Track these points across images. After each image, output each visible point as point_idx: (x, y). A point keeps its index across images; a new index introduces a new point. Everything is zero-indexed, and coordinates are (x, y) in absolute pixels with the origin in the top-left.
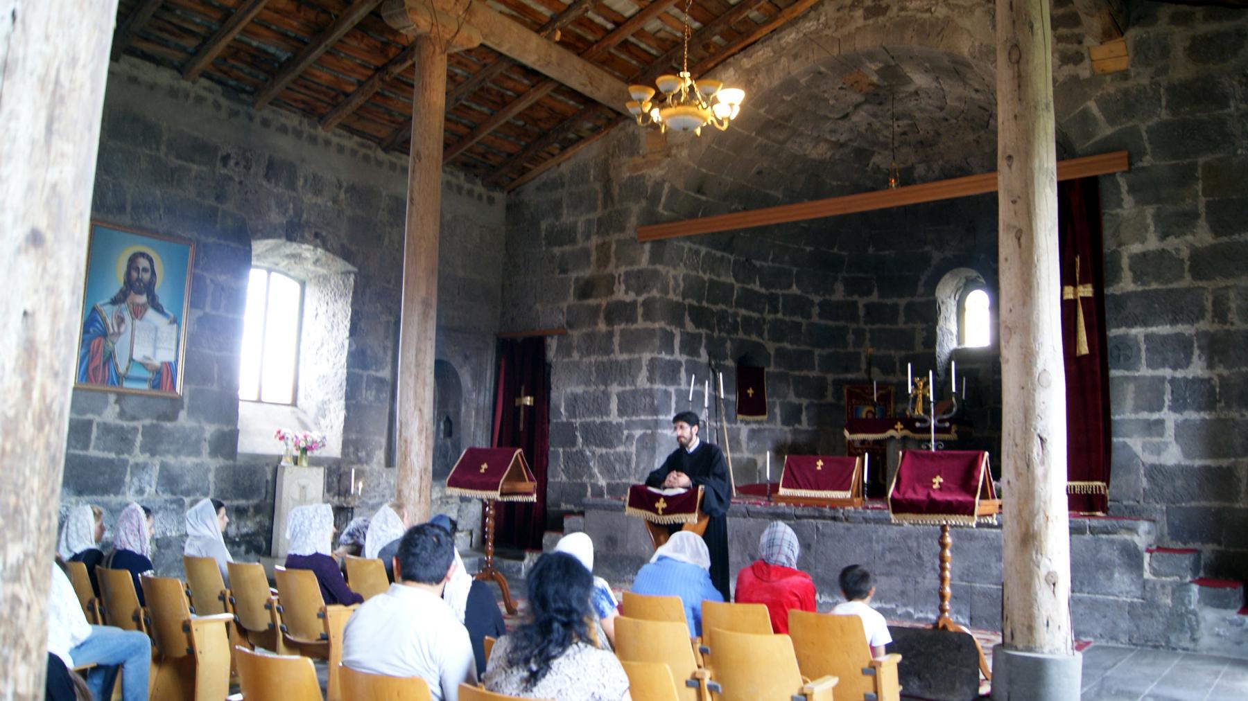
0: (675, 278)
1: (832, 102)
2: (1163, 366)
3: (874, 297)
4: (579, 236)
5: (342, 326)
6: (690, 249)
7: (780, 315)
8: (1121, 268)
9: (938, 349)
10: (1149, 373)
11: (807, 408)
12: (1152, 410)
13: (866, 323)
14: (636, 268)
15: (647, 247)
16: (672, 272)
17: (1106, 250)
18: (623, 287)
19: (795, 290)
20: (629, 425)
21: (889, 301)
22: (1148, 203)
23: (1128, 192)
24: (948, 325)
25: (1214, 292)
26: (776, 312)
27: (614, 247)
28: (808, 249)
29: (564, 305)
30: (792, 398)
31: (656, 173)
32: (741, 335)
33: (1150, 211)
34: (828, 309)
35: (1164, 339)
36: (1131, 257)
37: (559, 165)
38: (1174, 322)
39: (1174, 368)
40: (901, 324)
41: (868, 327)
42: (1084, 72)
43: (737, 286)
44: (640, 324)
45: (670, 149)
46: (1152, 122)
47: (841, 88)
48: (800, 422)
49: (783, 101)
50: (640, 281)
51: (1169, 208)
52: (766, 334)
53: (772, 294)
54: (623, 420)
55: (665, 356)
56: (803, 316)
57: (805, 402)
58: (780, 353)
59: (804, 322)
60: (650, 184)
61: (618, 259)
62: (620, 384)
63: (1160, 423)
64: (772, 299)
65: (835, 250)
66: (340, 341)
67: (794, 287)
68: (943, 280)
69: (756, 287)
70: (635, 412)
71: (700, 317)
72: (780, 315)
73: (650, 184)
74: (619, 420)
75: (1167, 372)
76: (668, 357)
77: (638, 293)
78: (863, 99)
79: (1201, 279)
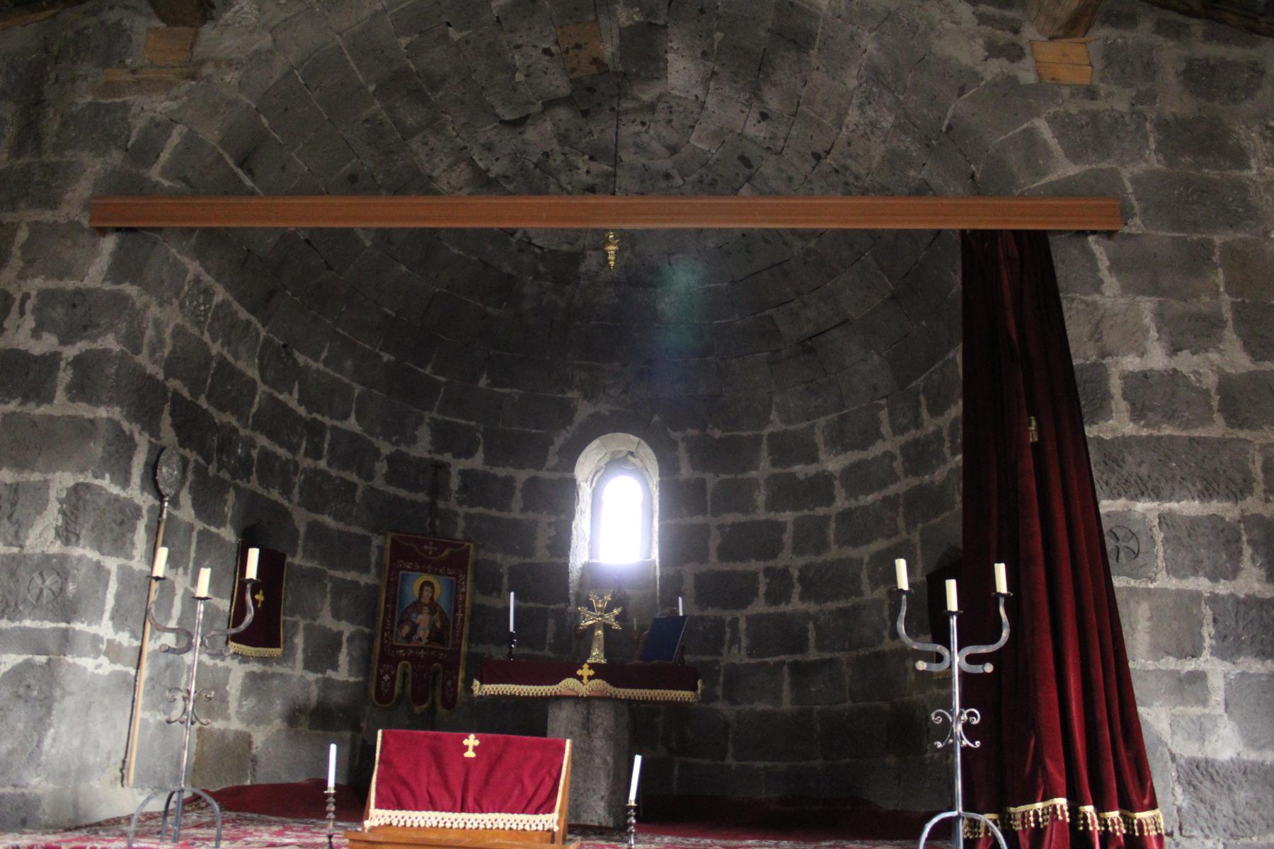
0: (158, 324)
1: (519, 77)
2: (1195, 572)
3: (477, 462)
6: (197, 280)
7: (322, 464)
8: (1107, 396)
9: (571, 560)
10: (1173, 584)
11: (351, 640)
12: (1182, 655)
13: (460, 503)
14: (70, 284)
15: (109, 244)
16: (154, 311)
18: (30, 322)
19: (352, 424)
21: (501, 472)
22: (1142, 292)
23: (1110, 269)
24: (581, 525)
25: (1263, 448)
26: (318, 456)
27: (23, 235)
28: (386, 357)
30: (327, 620)
31: (152, 106)
32: (254, 484)
34: (400, 468)
35: (1193, 524)
36: (1127, 377)
38: (1206, 494)
39: (1214, 577)
41: (462, 510)
43: (262, 388)
45: (202, 63)
46: (1139, 168)
47: (547, 52)
48: (335, 667)
49: (445, 37)
50: (77, 314)
51: (1177, 306)
52: (296, 490)
53: (314, 420)
55: (107, 484)
56: (359, 474)
57: (346, 628)
58: (315, 531)
59: (361, 484)
60: (139, 124)
61: (29, 263)
63: (1198, 678)
65: (428, 371)
67: (353, 419)
68: (588, 449)
69: (291, 400)
71: (192, 427)
72: (322, 464)
73: (139, 124)
75: (1201, 584)
76: (115, 490)
78: (565, 90)
79: (1241, 427)
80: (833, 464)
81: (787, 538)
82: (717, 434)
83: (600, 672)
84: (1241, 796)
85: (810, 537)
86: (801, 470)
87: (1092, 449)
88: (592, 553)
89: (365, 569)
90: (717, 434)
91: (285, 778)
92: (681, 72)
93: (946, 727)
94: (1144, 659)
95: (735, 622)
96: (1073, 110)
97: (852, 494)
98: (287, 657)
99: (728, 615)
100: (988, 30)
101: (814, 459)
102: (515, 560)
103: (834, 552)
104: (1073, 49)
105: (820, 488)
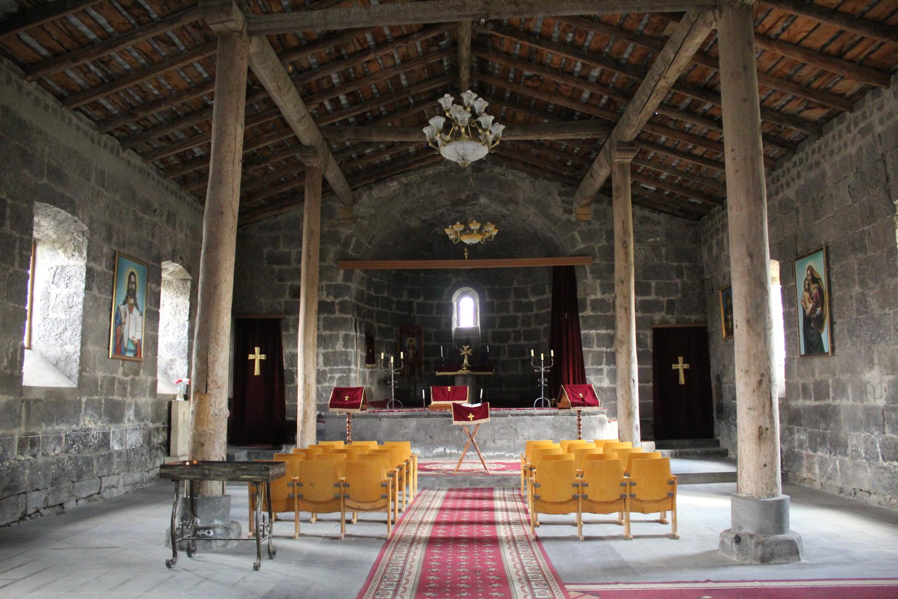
3: (421, 300)
4: (292, 260)
5: (183, 313)
8: (586, 305)
10: (598, 349)
14: (334, 283)
15: (342, 272)
17: (579, 297)
18: (325, 293)
19: (386, 294)
20: (331, 371)
21: (428, 302)
29: (283, 301)
31: (345, 232)
37: (276, 216)
38: (607, 329)
40: (434, 315)
41: (418, 315)
42: (573, 218)
44: (337, 315)
46: (600, 245)
51: (605, 282)
54: (327, 369)
60: (343, 237)
62: (324, 348)
63: (601, 370)
64: (377, 298)
66: (182, 321)
70: (335, 364)
74: (325, 368)
75: (604, 349)
77: (336, 297)
80: (533, 299)
81: (520, 321)
82: (497, 287)
83: (468, 368)
85: (526, 322)
86: (523, 300)
87: (581, 321)
88: (458, 324)
90: (497, 287)
91: (379, 400)
92: (483, 200)
93: (540, 383)
94: (588, 366)
95: (504, 347)
97: (539, 309)
99: (502, 345)
100: (564, 205)
101: (527, 297)
103: (533, 327)
104: (587, 210)
105: (529, 306)
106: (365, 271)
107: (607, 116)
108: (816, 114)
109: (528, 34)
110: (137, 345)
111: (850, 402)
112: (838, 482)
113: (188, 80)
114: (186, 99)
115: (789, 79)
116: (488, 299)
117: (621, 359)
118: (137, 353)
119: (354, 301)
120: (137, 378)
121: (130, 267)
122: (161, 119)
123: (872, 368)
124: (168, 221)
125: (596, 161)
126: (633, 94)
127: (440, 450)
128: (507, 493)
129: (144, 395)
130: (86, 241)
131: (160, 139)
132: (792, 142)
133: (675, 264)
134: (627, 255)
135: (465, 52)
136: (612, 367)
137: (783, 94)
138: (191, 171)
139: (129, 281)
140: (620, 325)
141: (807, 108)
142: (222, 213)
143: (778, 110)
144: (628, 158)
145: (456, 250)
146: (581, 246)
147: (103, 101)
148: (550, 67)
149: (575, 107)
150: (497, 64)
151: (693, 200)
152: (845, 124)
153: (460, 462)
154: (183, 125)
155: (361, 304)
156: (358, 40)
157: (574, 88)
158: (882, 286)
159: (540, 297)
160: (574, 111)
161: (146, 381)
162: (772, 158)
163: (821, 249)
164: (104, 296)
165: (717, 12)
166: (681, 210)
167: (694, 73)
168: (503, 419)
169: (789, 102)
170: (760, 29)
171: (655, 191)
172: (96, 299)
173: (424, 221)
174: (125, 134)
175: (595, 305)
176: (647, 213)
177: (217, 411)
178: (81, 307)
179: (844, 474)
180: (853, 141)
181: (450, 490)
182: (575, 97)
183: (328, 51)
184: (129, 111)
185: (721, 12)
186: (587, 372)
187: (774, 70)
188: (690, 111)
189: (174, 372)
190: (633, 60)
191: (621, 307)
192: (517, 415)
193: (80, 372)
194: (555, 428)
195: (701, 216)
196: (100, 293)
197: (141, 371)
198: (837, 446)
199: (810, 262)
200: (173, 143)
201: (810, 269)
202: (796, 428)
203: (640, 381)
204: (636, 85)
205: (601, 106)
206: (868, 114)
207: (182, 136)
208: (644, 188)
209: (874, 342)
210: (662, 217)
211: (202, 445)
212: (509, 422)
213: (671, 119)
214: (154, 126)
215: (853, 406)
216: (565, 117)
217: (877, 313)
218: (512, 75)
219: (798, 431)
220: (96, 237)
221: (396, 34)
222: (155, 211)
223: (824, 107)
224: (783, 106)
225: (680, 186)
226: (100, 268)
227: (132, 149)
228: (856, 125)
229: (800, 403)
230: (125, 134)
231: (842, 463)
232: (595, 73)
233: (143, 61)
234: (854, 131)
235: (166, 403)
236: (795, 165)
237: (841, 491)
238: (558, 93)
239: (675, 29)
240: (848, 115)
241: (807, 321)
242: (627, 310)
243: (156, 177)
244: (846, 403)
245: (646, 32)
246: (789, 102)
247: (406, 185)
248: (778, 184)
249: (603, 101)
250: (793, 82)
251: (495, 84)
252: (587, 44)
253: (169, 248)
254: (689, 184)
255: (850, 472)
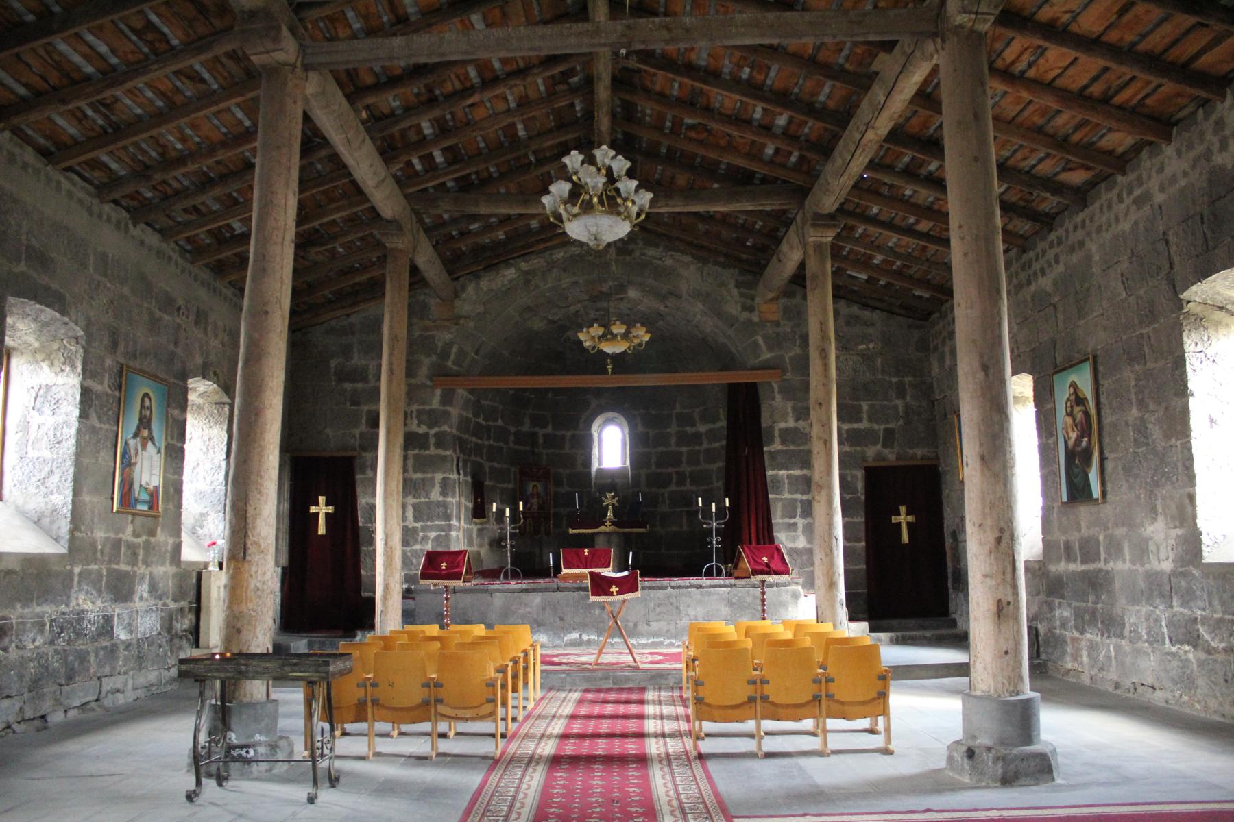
3: (549, 430)
4: (370, 377)
5: (217, 450)
14: (427, 407)
15: (438, 392)
17: (764, 425)
18: (415, 422)
19: (500, 422)
20: (424, 529)
29: (357, 432)
31: (444, 337)
33: (789, 405)
35: (797, 478)
36: (780, 430)
37: (348, 315)
38: (802, 468)
39: (802, 494)
40: (567, 450)
41: (545, 451)
44: (432, 451)
46: (791, 354)
51: (800, 404)
54: (419, 525)
58: (491, 468)
60: (440, 344)
62: (414, 497)
63: (795, 524)
64: (488, 428)
66: (216, 461)
70: (430, 519)
73: (440, 344)
74: (415, 525)
75: (798, 496)
77: (430, 428)
80: (702, 428)
83: (613, 523)
84: (804, 557)
86: (688, 429)
87: (766, 457)
88: (600, 463)
89: (509, 482)
90: (653, 412)
92: (633, 293)
93: (711, 543)
94: (777, 519)
95: (663, 494)
96: (770, 331)
98: (488, 522)
100: (742, 300)
101: (693, 425)
102: (568, 471)
105: (697, 438)
106: (472, 391)
107: (799, 180)
108: (1077, 177)
109: (689, 69)
110: (153, 494)
111: (1127, 566)
112: (1113, 674)
113: (224, 130)
114: (222, 155)
115: (1040, 130)
116: (640, 428)
117: (819, 509)
118: (153, 505)
119: (454, 431)
120: (152, 540)
121: (143, 387)
122: (186, 183)
123: (1155, 519)
124: (197, 323)
125: (784, 241)
126: (832, 150)
127: (575, 635)
128: (664, 695)
129: (163, 564)
130: (81, 351)
131: (185, 210)
132: (1047, 214)
133: (894, 380)
134: (826, 367)
135: (603, 92)
136: (809, 520)
137: (1033, 151)
138: (229, 254)
139: (142, 407)
140: (818, 463)
141: (1064, 170)
142: (267, 313)
143: (1028, 172)
144: (828, 237)
145: (597, 362)
146: (767, 355)
147: (105, 158)
148: (720, 114)
149: (754, 167)
150: (648, 109)
151: (917, 293)
152: (1116, 191)
153: (600, 653)
154: (218, 191)
155: (465, 436)
156: (458, 77)
157: (753, 142)
158: (1166, 408)
159: (711, 426)
160: (755, 172)
161: (166, 544)
162: (1021, 236)
163: (1087, 359)
164: (107, 426)
165: (939, 40)
166: (901, 306)
167: (914, 121)
168: (661, 593)
169: (1041, 160)
170: (999, 64)
171: (867, 281)
172: (94, 430)
173: (552, 322)
174: (135, 203)
175: (787, 436)
176: (855, 309)
177: (259, 585)
178: (73, 441)
179: (1121, 664)
180: (1126, 215)
181: (587, 691)
182: (755, 153)
183: (416, 90)
184: (143, 171)
185: (943, 41)
186: (775, 528)
187: (1020, 119)
188: (910, 173)
189: (206, 530)
190: (831, 104)
191: (819, 438)
192: (680, 587)
193: (72, 532)
194: (731, 604)
195: (930, 314)
196: (100, 422)
197: (159, 529)
198: (1111, 625)
199: (1073, 377)
200: (204, 215)
201: (1074, 385)
202: (1057, 601)
203: (846, 538)
204: (836, 138)
205: (789, 165)
206: (1144, 177)
207: (216, 207)
208: (851, 276)
209: (1156, 484)
210: (876, 316)
211: (239, 631)
212: (669, 597)
213: (885, 184)
214: (176, 193)
215: (1130, 571)
216: (741, 181)
217: (1161, 444)
218: (668, 124)
219: (1060, 605)
220: (96, 344)
221: (509, 68)
222: (179, 309)
223: (1088, 168)
224: (1034, 166)
225: (899, 274)
226: (102, 387)
227: (148, 224)
228: (1130, 193)
229: (1062, 567)
230: (135, 203)
231: (1118, 648)
232: (781, 121)
233: (160, 104)
234: (1128, 201)
235: (194, 574)
236: (1051, 245)
237: (1117, 686)
238: (731, 147)
239: (885, 63)
240: (1119, 178)
241: (1070, 455)
242: (827, 442)
243: (180, 260)
244: (1121, 566)
245: (847, 66)
246: (1041, 160)
247: (527, 273)
248: (1031, 272)
249: (793, 159)
250: (1047, 135)
251: (647, 136)
252: (769, 82)
253: (199, 360)
254: (911, 272)
255: (1128, 660)
